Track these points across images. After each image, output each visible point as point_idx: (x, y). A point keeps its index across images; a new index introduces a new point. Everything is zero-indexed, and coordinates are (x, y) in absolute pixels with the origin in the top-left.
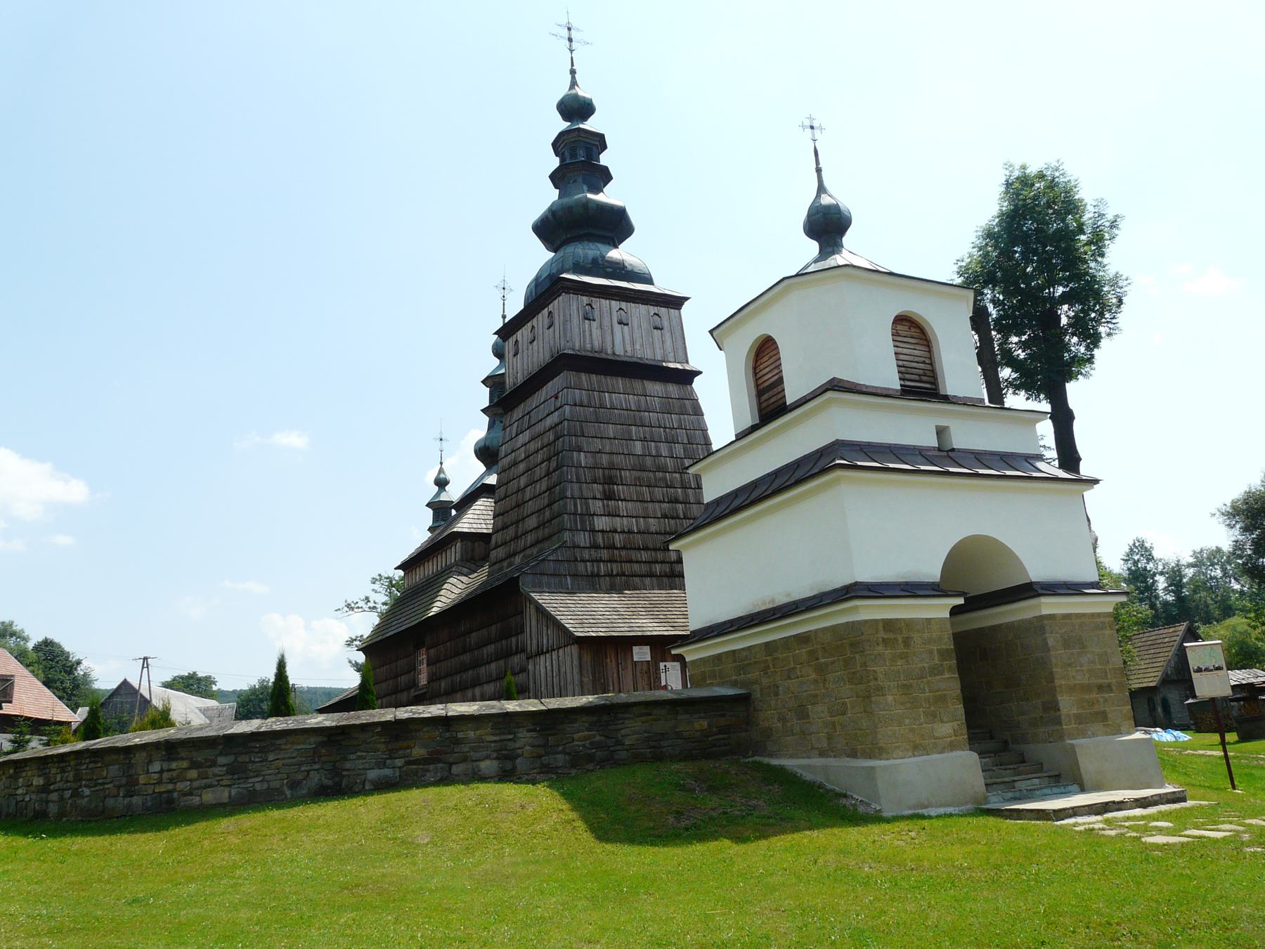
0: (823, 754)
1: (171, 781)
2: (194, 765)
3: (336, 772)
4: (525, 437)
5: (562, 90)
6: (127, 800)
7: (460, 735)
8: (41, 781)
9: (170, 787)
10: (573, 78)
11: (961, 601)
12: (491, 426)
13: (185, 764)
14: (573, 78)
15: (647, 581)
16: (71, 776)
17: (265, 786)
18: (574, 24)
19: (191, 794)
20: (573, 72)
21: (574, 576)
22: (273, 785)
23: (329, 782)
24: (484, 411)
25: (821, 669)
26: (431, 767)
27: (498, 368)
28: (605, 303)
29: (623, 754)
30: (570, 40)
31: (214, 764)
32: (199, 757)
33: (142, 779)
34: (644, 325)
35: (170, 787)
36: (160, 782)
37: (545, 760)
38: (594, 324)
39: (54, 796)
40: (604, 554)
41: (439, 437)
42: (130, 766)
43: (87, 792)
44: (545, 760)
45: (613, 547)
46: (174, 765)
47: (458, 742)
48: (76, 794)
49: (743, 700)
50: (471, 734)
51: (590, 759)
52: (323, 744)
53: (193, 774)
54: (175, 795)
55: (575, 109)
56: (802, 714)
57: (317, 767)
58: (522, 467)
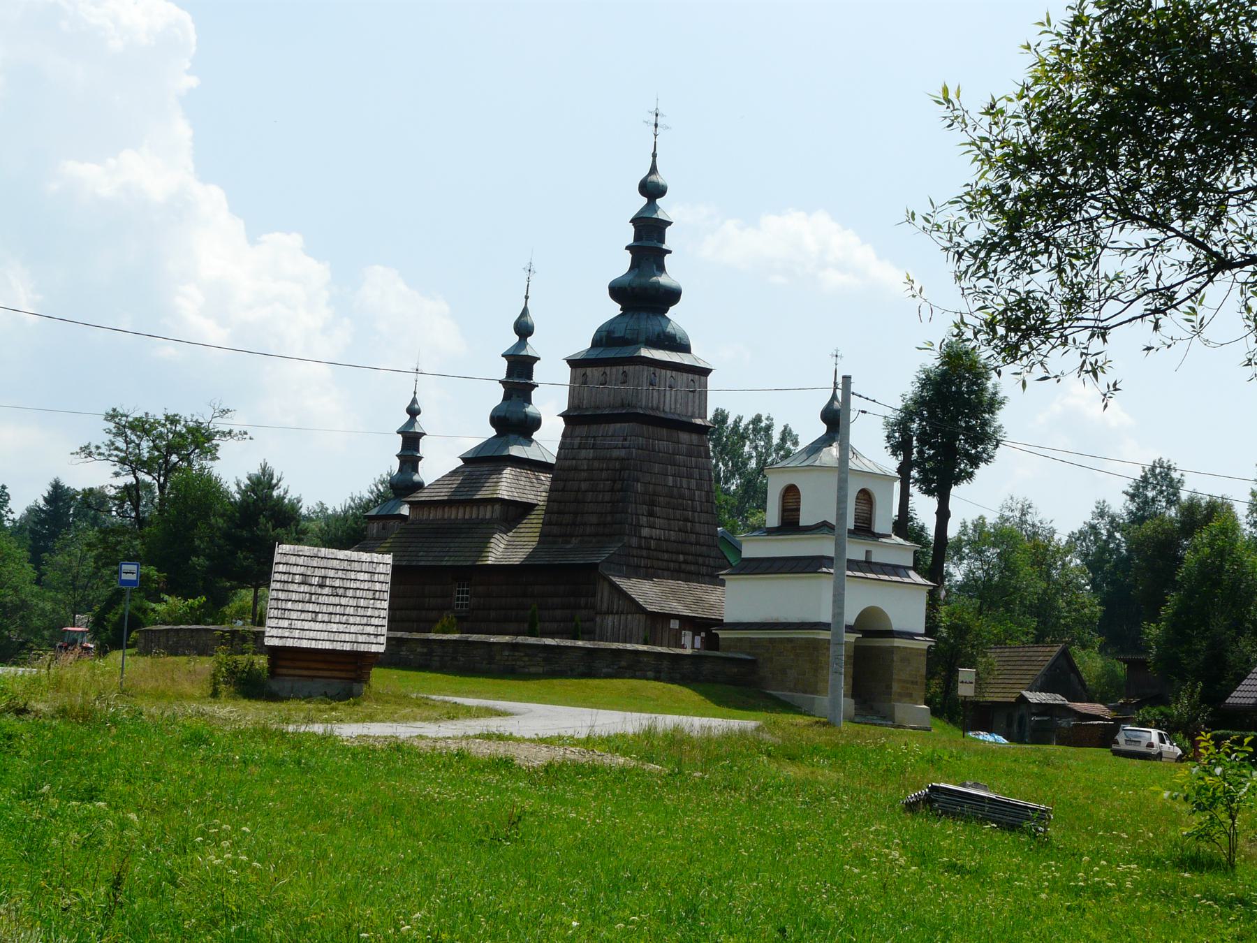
4: (591, 453)
10: (654, 161)
12: (506, 398)
14: (654, 161)
15: (666, 573)
18: (660, 111)
20: (654, 155)
21: (628, 566)
28: (663, 371)
30: (656, 125)
40: (644, 553)
41: (422, 368)
45: (649, 549)
58: (584, 475)
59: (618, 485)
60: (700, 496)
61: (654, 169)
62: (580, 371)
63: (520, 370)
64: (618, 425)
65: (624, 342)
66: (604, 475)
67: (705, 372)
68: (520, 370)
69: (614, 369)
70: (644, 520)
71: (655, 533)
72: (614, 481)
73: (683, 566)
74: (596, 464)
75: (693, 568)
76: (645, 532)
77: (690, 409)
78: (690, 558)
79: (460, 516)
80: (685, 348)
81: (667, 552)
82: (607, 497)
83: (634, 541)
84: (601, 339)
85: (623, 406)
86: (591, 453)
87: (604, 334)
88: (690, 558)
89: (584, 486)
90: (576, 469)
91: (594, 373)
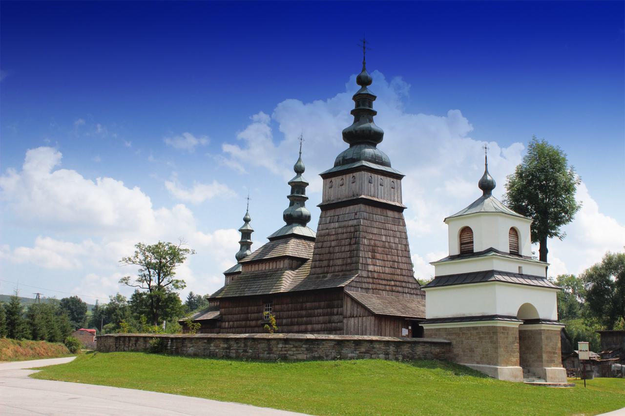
0: (478, 363)
1: (285, 351)
2: (294, 347)
6: (268, 355)
9: (286, 353)
13: (292, 346)
16: (243, 345)
24: (288, 197)
29: (417, 357)
31: (301, 347)
33: (275, 349)
35: (286, 353)
36: (281, 351)
37: (397, 356)
42: (269, 345)
43: (250, 351)
44: (397, 356)
46: (287, 346)
47: (374, 348)
48: (245, 351)
49: (449, 344)
53: (295, 349)
56: (472, 350)
59: (353, 241)
66: (345, 236)
67: (399, 177)
69: (348, 176)
70: (369, 261)
73: (394, 288)
76: (371, 268)
79: (267, 268)
80: (388, 165)
81: (384, 280)
82: (347, 248)
83: (364, 274)
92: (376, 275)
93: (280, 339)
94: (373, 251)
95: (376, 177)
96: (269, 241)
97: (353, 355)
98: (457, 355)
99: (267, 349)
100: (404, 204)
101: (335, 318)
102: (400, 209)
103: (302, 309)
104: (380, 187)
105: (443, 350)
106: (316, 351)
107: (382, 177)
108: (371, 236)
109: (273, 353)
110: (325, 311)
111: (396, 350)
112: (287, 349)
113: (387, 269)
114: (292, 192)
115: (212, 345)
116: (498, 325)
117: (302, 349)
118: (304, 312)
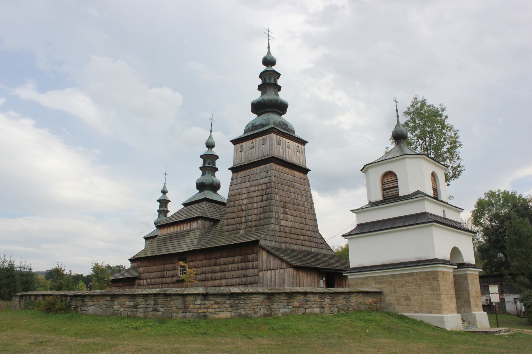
0: (416, 312)
1: (205, 308)
2: (216, 303)
3: (270, 309)
4: (248, 184)
5: (265, 54)
6: (183, 314)
7: (309, 299)
8: (132, 303)
9: (205, 310)
11: (456, 267)
13: (212, 302)
16: (152, 302)
17: (245, 312)
18: (270, 30)
19: (215, 314)
20: (269, 48)
22: (249, 312)
23: (266, 313)
24: (201, 168)
25: (418, 285)
26: (300, 309)
27: (207, 151)
30: (269, 35)
31: (225, 303)
32: (218, 300)
33: (191, 307)
34: (295, 150)
35: (205, 310)
36: (200, 308)
37: (332, 309)
38: (281, 147)
39: (141, 310)
43: (162, 309)
44: (332, 309)
46: (207, 302)
47: (308, 301)
48: (156, 310)
49: (380, 293)
50: (312, 299)
51: (343, 309)
52: (266, 299)
54: (208, 314)
55: (269, 62)
56: (408, 298)
57: (263, 307)
58: (244, 196)
59: (265, 197)
60: (307, 205)
61: (269, 53)
62: (239, 145)
63: (209, 163)
64: (262, 166)
65: (263, 126)
66: (256, 194)
68: (209, 163)
69: (257, 139)
70: (281, 216)
71: (289, 224)
72: (263, 196)
73: (304, 242)
74: (252, 189)
75: (308, 243)
76: (283, 223)
77: (298, 161)
78: (306, 238)
81: (295, 234)
82: (259, 205)
83: (277, 228)
84: (249, 129)
85: (264, 156)
86: (248, 184)
87: (250, 126)
88: (306, 238)
89: (245, 202)
90: (240, 194)
91: (246, 144)
92: (287, 229)
93: (198, 294)
94: (284, 207)
95: (283, 139)
96: (183, 206)
97: (286, 310)
98: (390, 305)
99: (182, 307)
100: (308, 167)
101: (250, 272)
102: (305, 171)
103: (215, 265)
104: (287, 149)
105: (375, 300)
106: (243, 308)
107: (289, 141)
108: (282, 193)
109: (189, 312)
110: (240, 265)
111: (331, 303)
112: (207, 306)
113: (297, 224)
114: (204, 163)
115: (116, 303)
116: (440, 269)
117: (226, 305)
118: (217, 268)
